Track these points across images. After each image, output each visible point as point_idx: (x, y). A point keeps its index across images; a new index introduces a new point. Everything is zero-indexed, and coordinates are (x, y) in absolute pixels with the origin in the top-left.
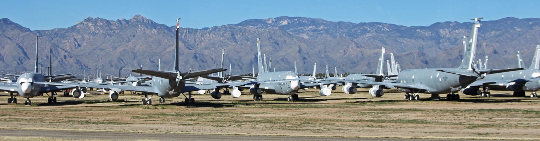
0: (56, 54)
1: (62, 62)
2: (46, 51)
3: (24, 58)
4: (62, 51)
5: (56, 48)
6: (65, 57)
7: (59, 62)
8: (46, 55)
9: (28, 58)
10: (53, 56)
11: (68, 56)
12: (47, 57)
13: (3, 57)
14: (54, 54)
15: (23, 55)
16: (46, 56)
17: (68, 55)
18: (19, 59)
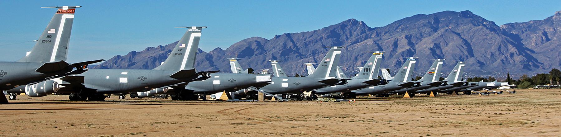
0: (504, 52)
1: (506, 60)
2: (493, 48)
3: (467, 56)
4: (512, 48)
5: (507, 44)
6: (512, 55)
7: (502, 60)
8: (491, 52)
9: (472, 56)
10: (500, 54)
11: (516, 53)
12: (492, 55)
13: (444, 56)
14: (502, 51)
15: (466, 53)
16: (490, 54)
17: (515, 53)
18: (461, 57)
